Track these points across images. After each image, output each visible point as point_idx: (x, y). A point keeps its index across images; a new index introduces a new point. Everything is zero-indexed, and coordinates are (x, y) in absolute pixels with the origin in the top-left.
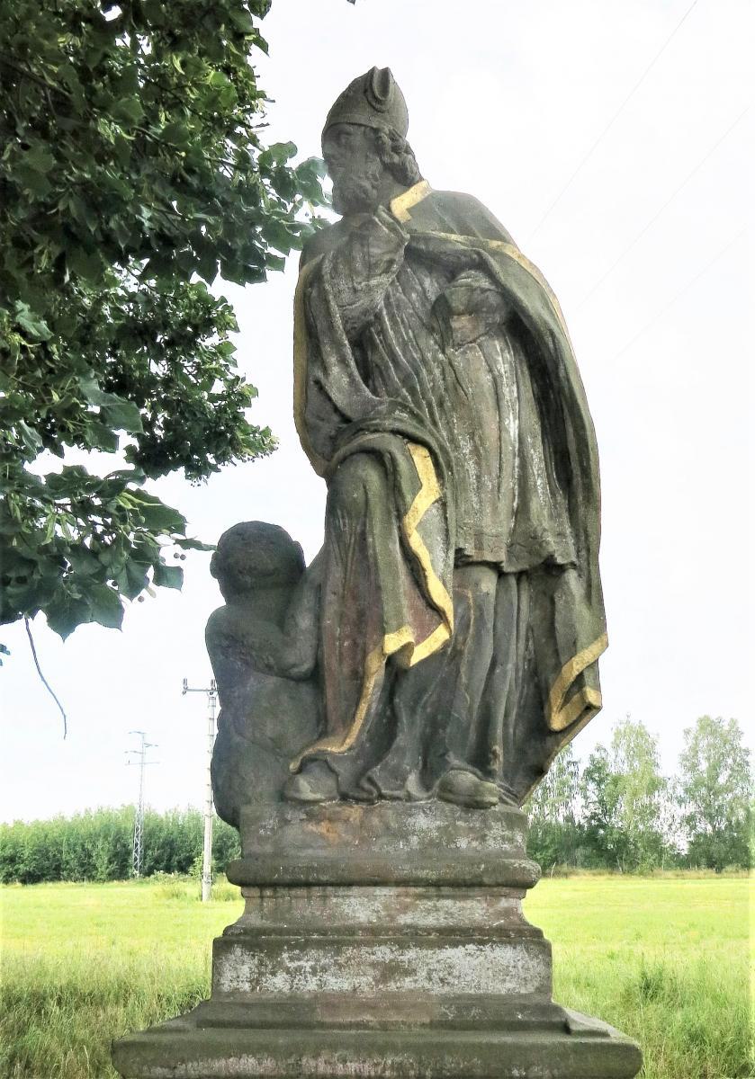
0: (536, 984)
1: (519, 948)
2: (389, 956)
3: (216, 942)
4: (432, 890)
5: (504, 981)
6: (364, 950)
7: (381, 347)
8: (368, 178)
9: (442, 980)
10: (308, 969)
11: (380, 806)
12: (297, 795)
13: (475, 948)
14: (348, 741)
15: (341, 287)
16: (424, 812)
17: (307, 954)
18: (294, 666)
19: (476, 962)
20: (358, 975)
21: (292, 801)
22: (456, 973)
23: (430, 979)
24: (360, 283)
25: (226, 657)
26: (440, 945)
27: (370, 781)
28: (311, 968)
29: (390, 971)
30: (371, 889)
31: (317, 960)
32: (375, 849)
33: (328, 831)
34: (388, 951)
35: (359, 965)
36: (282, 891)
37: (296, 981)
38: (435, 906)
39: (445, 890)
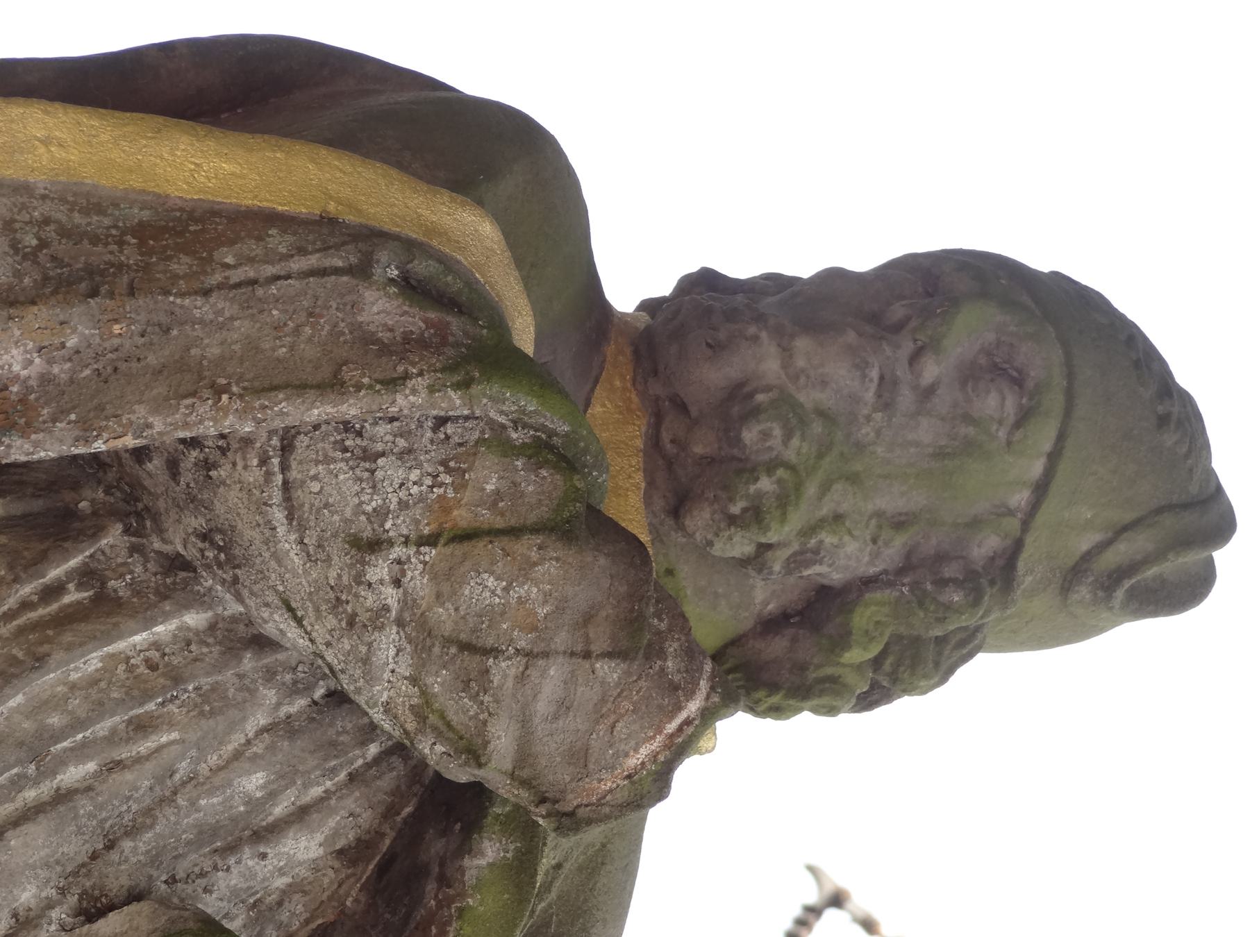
7: (27, 590)
8: (810, 530)
15: (389, 470)
24: (397, 583)
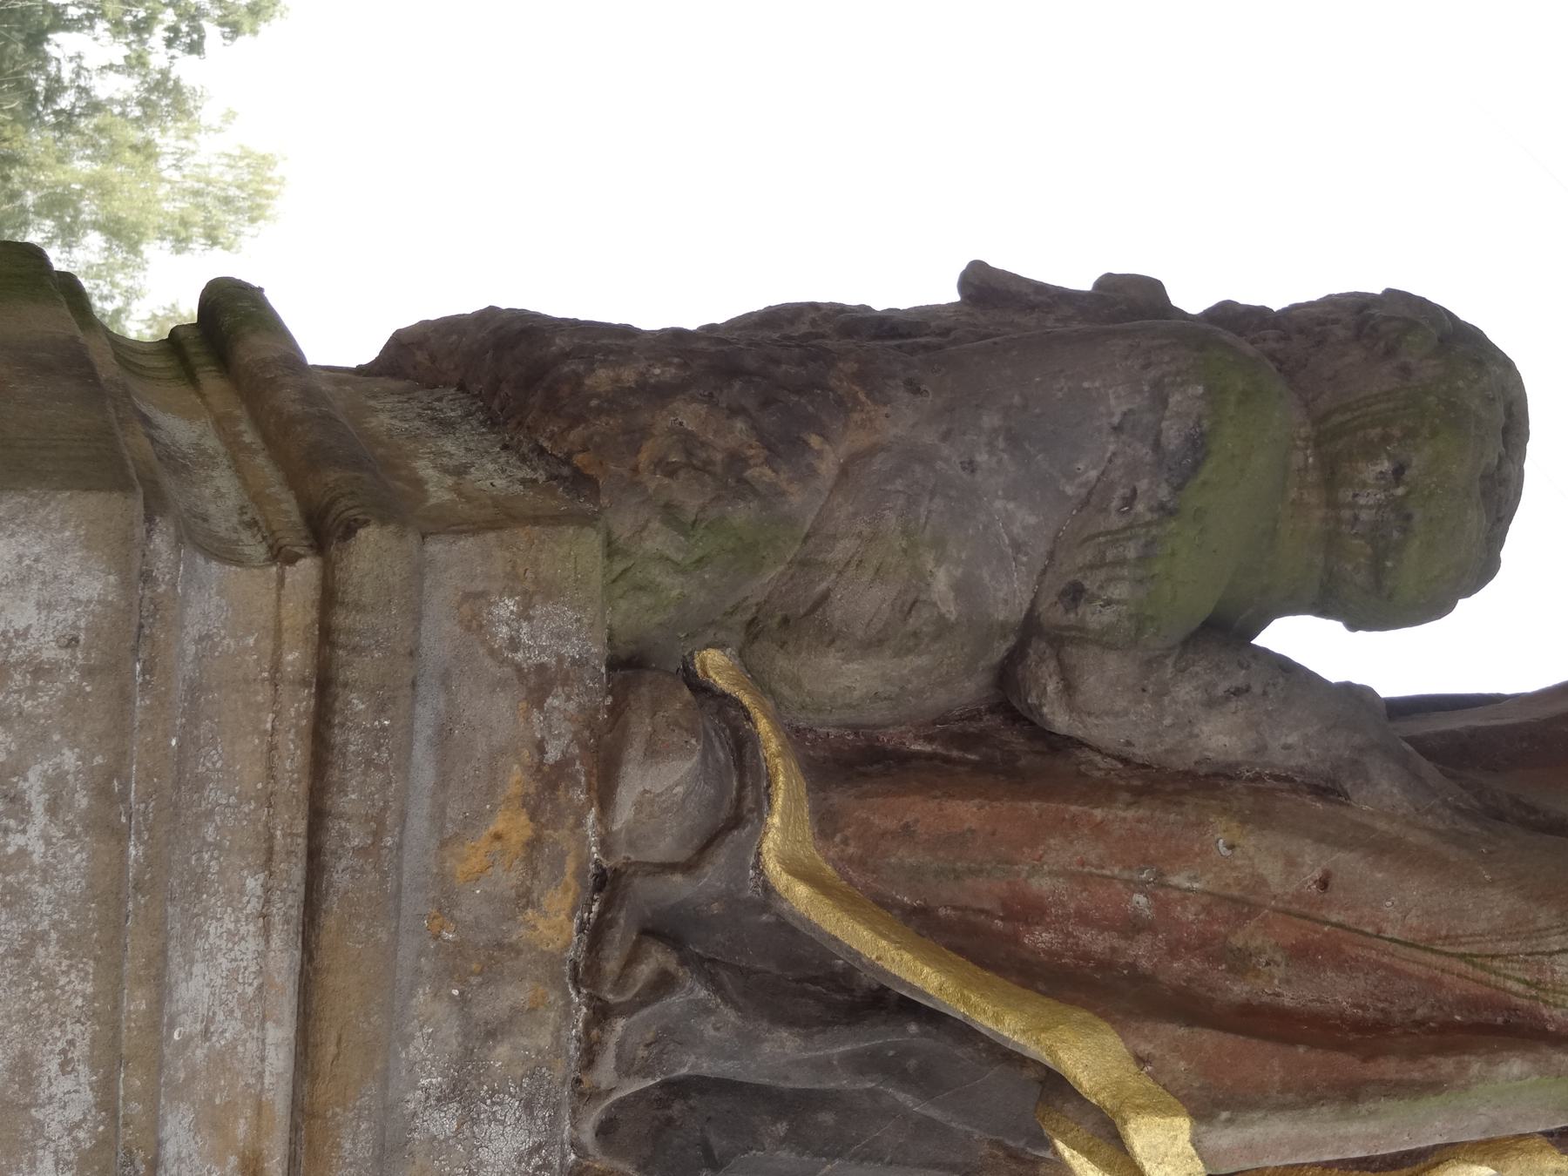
2: (54, 1120)
6: (81, 1034)
11: (569, 1002)
12: (635, 751)
14: (801, 891)
16: (536, 1149)
17: (71, 835)
18: (1069, 688)
21: (611, 710)
25: (1117, 429)
27: (663, 984)
28: (23, 852)
30: (286, 1006)
32: (422, 996)
33: (498, 837)
34: (74, 1114)
35: (27, 1016)
36: (299, 705)
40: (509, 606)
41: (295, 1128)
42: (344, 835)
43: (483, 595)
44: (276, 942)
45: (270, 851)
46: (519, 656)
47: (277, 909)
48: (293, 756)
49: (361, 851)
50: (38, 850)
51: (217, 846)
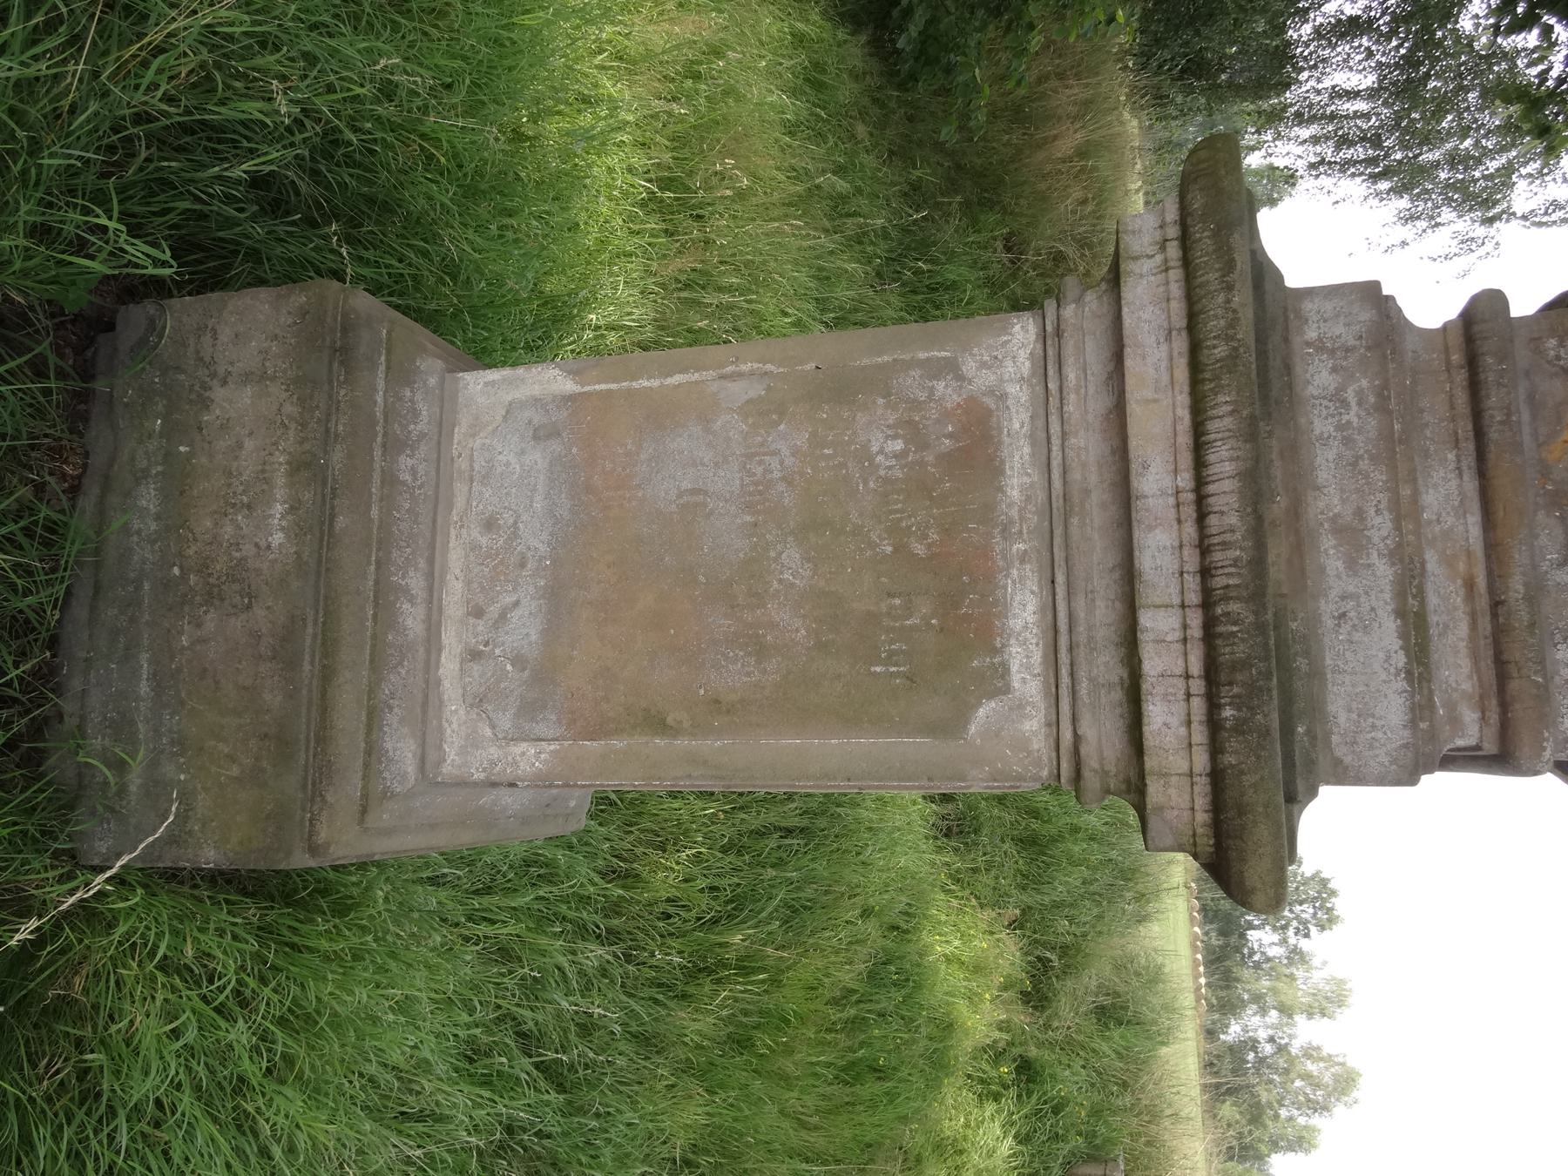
0: (1348, 760)
1: (1407, 733)
2: (1376, 536)
3: (1374, 286)
4: (1483, 602)
5: (1350, 710)
6: (1383, 497)
9: (1344, 615)
10: (1345, 418)
13: (1401, 665)
19: (1377, 667)
20: (1342, 491)
22: (1357, 636)
23: (1343, 598)
26: (1400, 613)
28: (1348, 422)
29: (1352, 535)
30: (1475, 506)
31: (1360, 430)
32: (1541, 515)
35: (1358, 491)
36: (1461, 377)
37: (1325, 403)
38: (1456, 609)
39: (1485, 624)
40: (1553, 342)
41: (1488, 557)
42: (1492, 417)
43: (1540, 338)
44: (1466, 478)
45: (1457, 441)
46: (1562, 362)
47: (1464, 464)
48: (1462, 398)
49: (1501, 423)
50: (1355, 420)
51: (1432, 439)
